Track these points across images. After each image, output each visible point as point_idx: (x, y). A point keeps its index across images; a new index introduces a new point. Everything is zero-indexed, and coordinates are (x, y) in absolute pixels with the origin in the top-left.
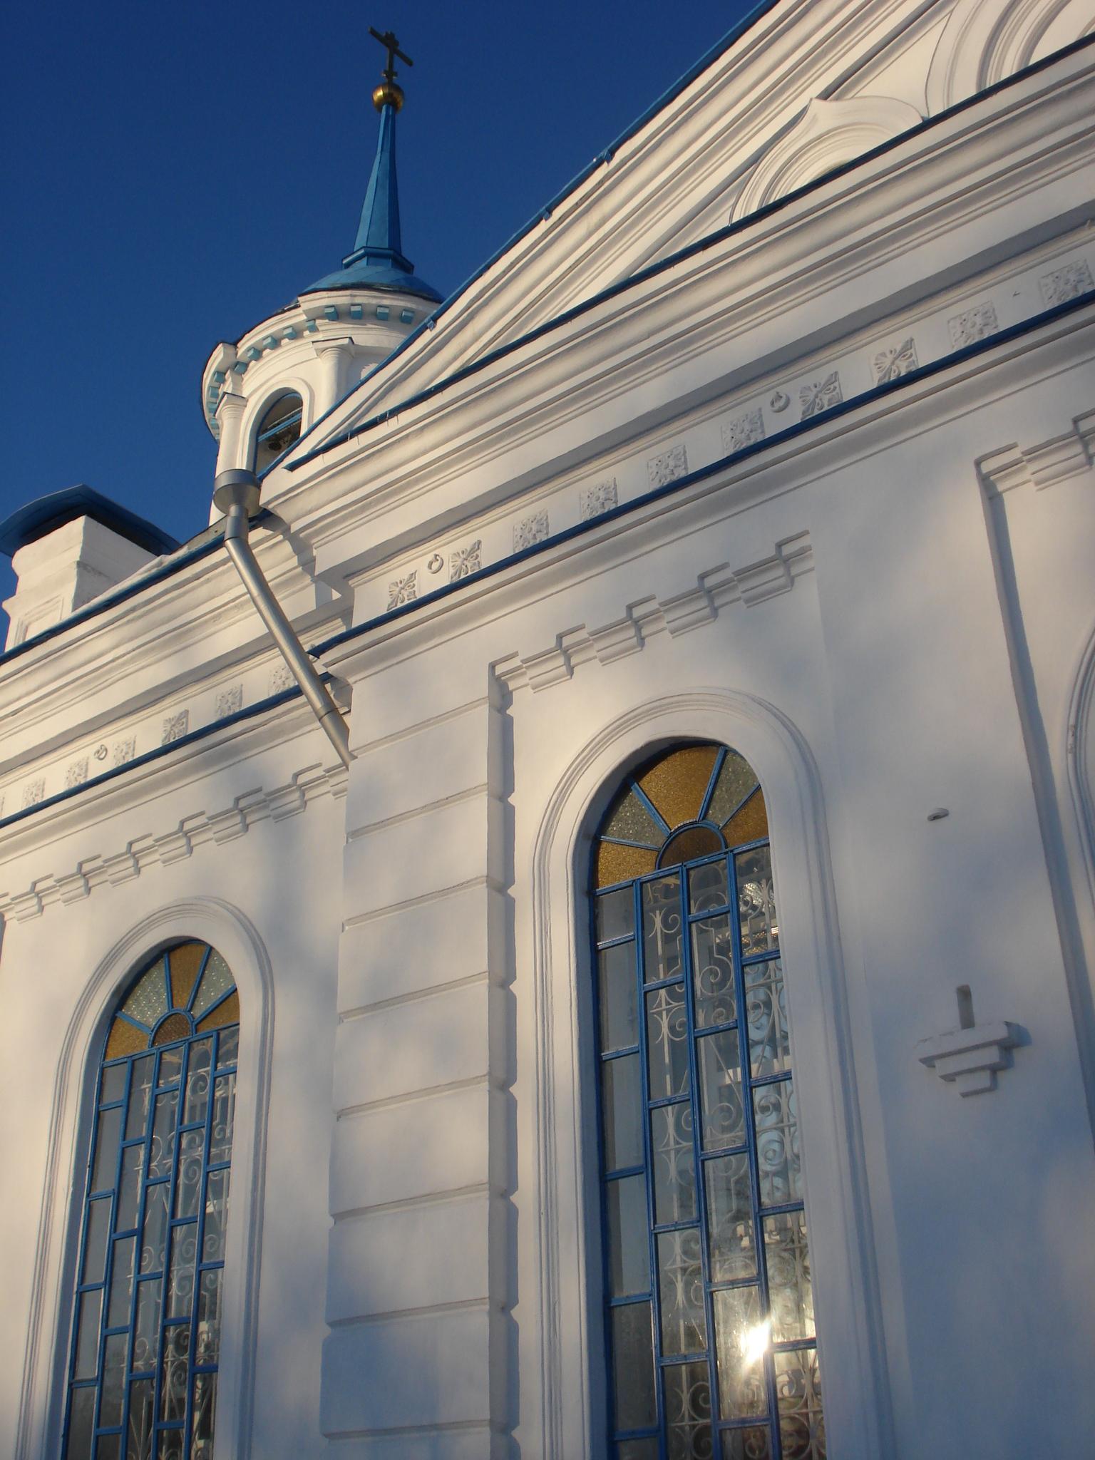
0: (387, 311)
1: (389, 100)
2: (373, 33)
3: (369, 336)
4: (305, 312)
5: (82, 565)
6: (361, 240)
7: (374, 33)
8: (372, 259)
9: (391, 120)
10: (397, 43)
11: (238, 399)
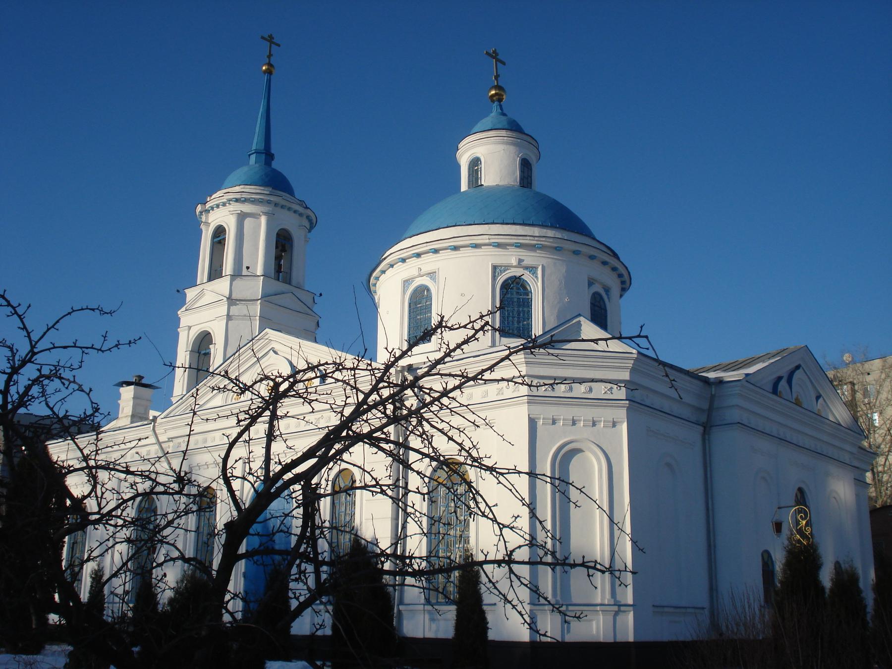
1: (269, 72)
2: (263, 38)
3: (247, 208)
6: (254, 147)
7: (263, 38)
9: (269, 82)
11: (207, 224)
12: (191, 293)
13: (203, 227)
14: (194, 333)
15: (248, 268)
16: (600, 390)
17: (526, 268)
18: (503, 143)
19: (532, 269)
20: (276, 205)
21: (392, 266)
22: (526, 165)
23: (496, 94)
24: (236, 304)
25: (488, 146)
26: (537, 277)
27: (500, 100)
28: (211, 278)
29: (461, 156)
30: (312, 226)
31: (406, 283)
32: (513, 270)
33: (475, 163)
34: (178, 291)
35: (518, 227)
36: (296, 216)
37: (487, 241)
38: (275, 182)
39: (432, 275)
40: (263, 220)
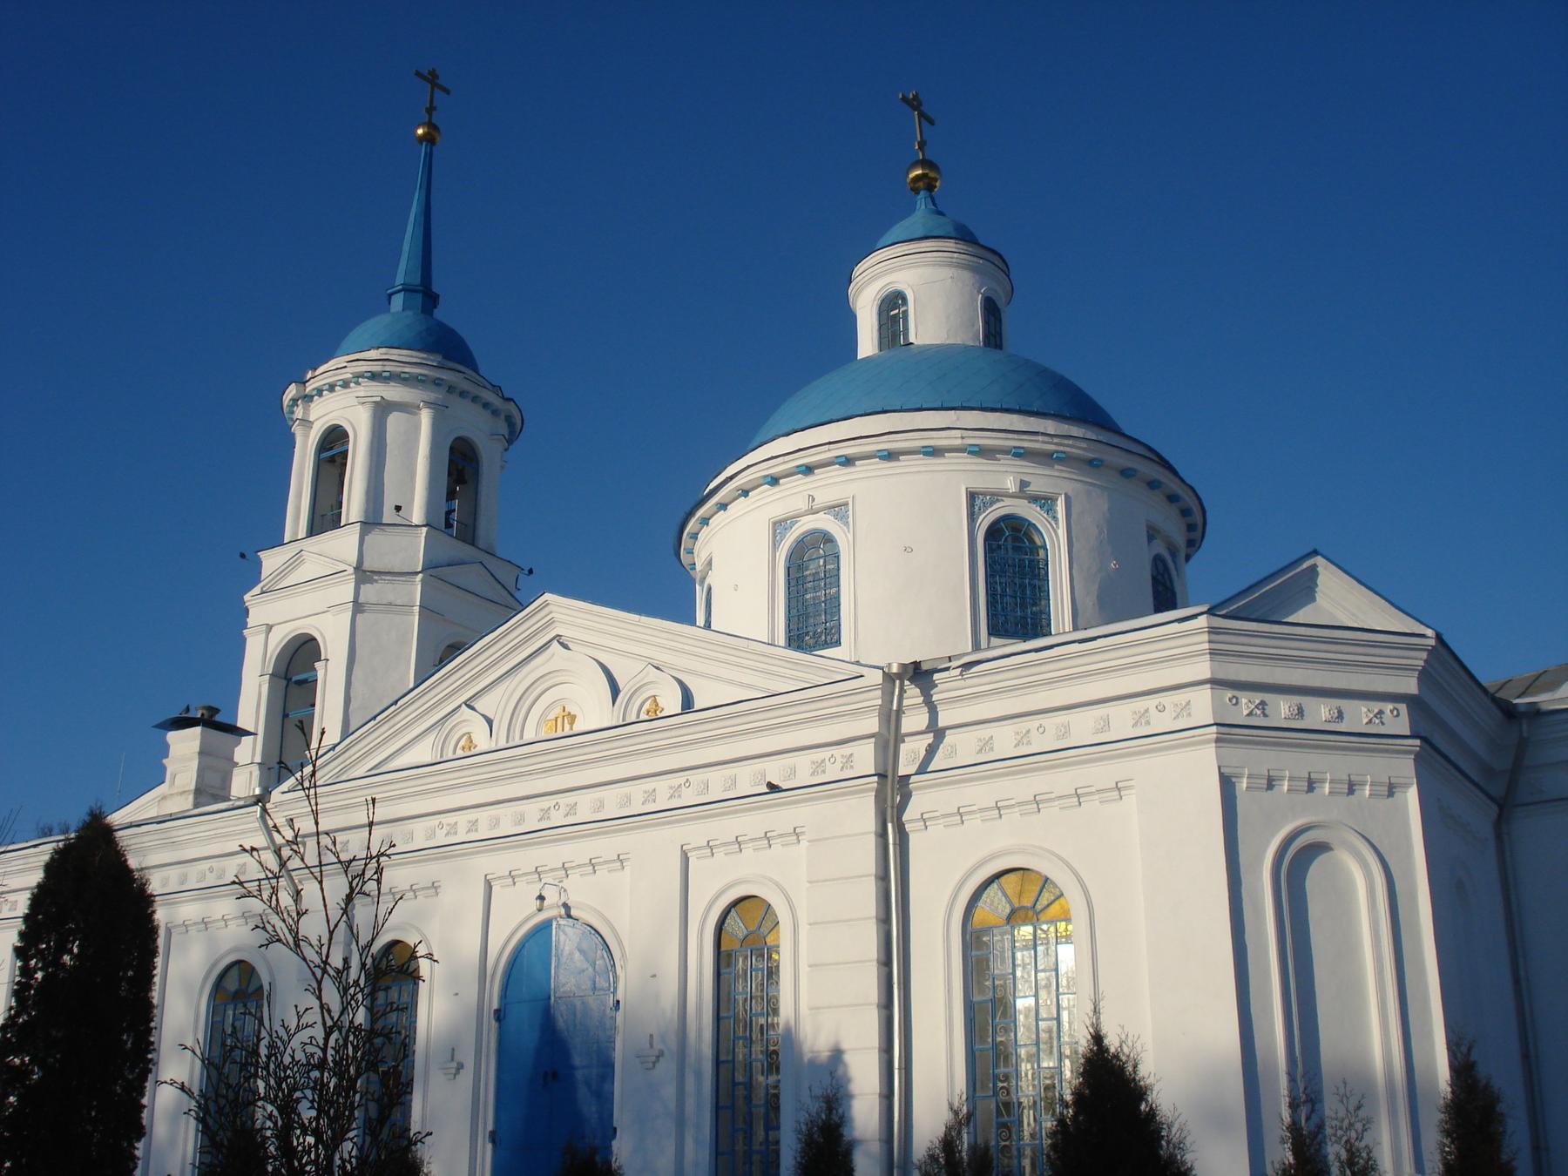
1: (429, 139)
2: (418, 74)
3: (394, 392)
5: (201, 753)
6: (400, 280)
7: (418, 74)
11: (306, 423)
12: (271, 560)
13: (297, 429)
14: (279, 638)
15: (398, 508)
16: (1360, 715)
17: (1034, 499)
18: (950, 265)
19: (1046, 502)
20: (451, 389)
21: (745, 493)
22: (991, 310)
23: (924, 176)
24: (371, 581)
25: (921, 271)
26: (1055, 518)
27: (930, 188)
28: (313, 531)
29: (859, 291)
30: (512, 435)
31: (779, 527)
32: (1008, 501)
33: (892, 305)
34: (243, 556)
35: (1015, 417)
36: (486, 414)
37: (958, 442)
38: (445, 346)
39: (839, 510)
40: (425, 417)
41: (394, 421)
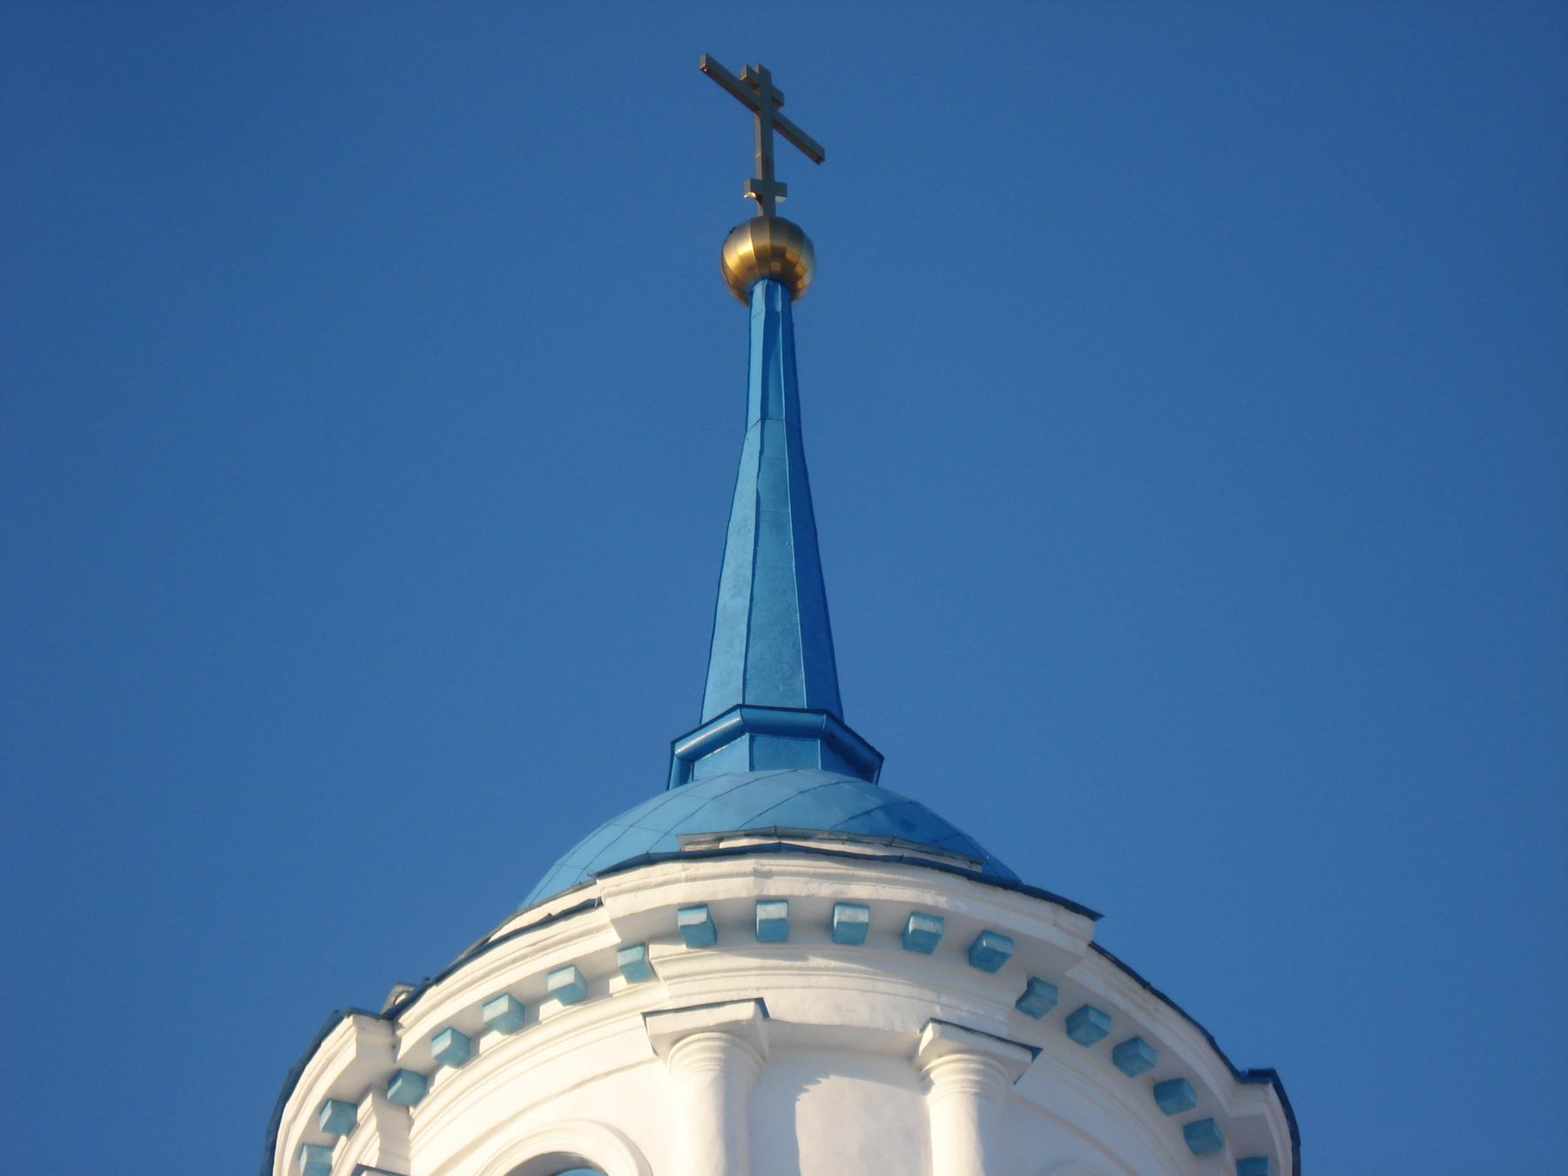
0: (863, 916)
1: (777, 272)
2: (714, 71)
4: (617, 923)
7: (714, 71)
8: (762, 740)
9: (780, 327)
10: (777, 100)
41: (823, 1114)
